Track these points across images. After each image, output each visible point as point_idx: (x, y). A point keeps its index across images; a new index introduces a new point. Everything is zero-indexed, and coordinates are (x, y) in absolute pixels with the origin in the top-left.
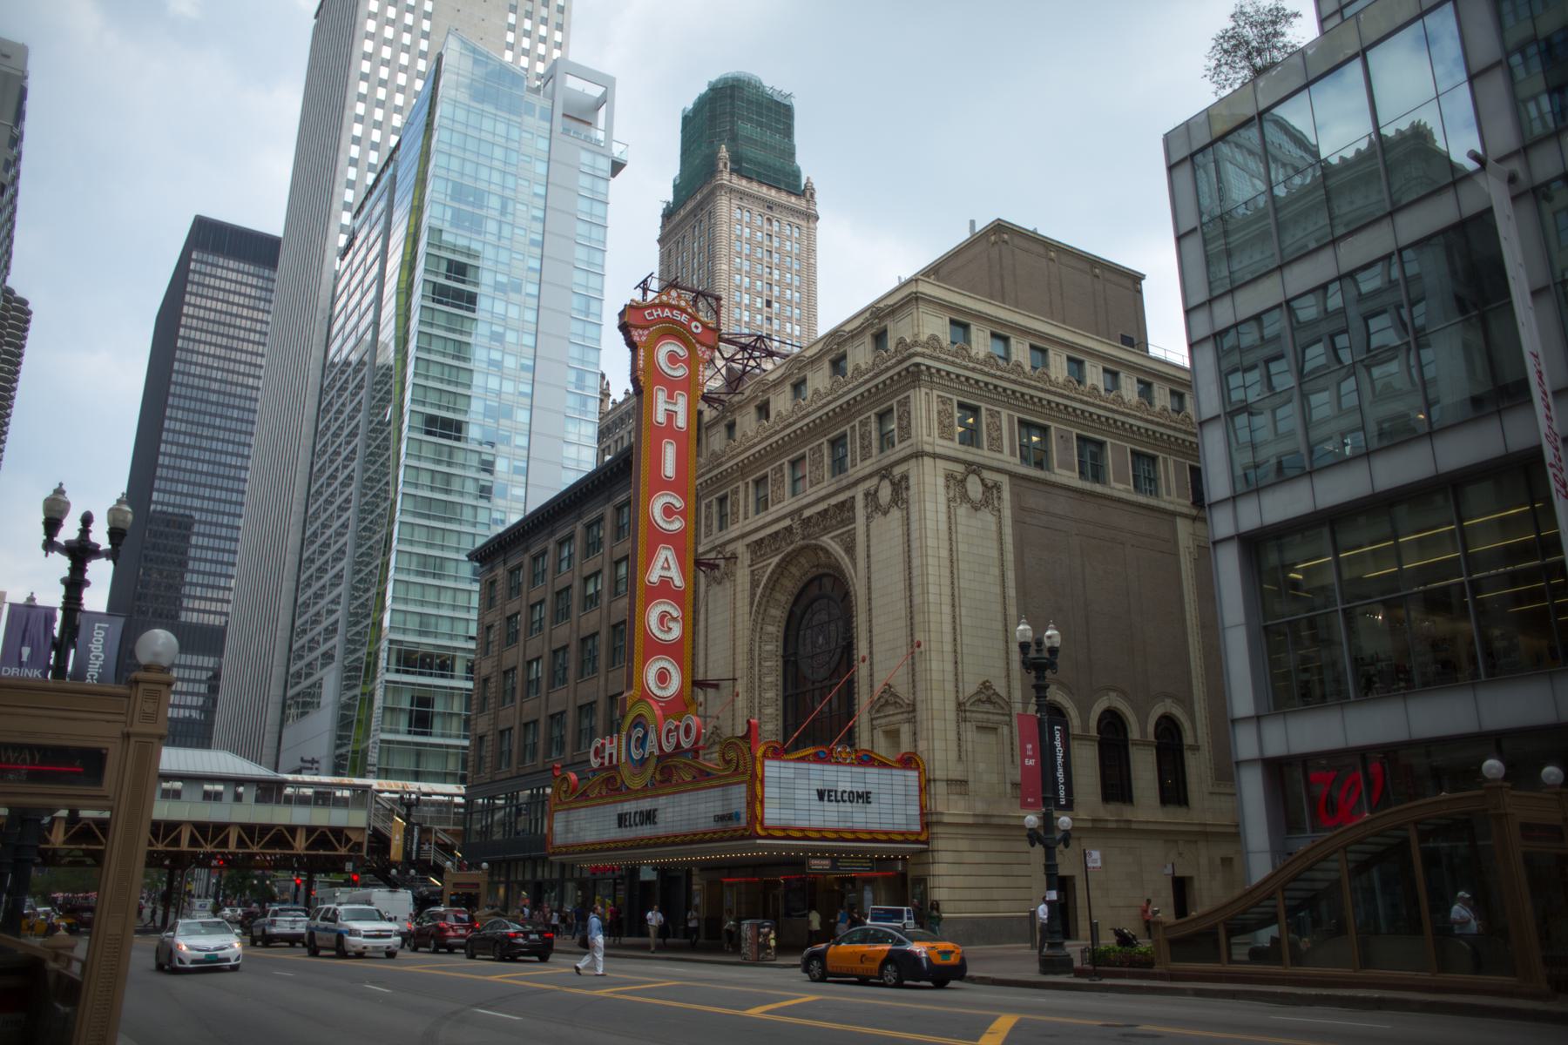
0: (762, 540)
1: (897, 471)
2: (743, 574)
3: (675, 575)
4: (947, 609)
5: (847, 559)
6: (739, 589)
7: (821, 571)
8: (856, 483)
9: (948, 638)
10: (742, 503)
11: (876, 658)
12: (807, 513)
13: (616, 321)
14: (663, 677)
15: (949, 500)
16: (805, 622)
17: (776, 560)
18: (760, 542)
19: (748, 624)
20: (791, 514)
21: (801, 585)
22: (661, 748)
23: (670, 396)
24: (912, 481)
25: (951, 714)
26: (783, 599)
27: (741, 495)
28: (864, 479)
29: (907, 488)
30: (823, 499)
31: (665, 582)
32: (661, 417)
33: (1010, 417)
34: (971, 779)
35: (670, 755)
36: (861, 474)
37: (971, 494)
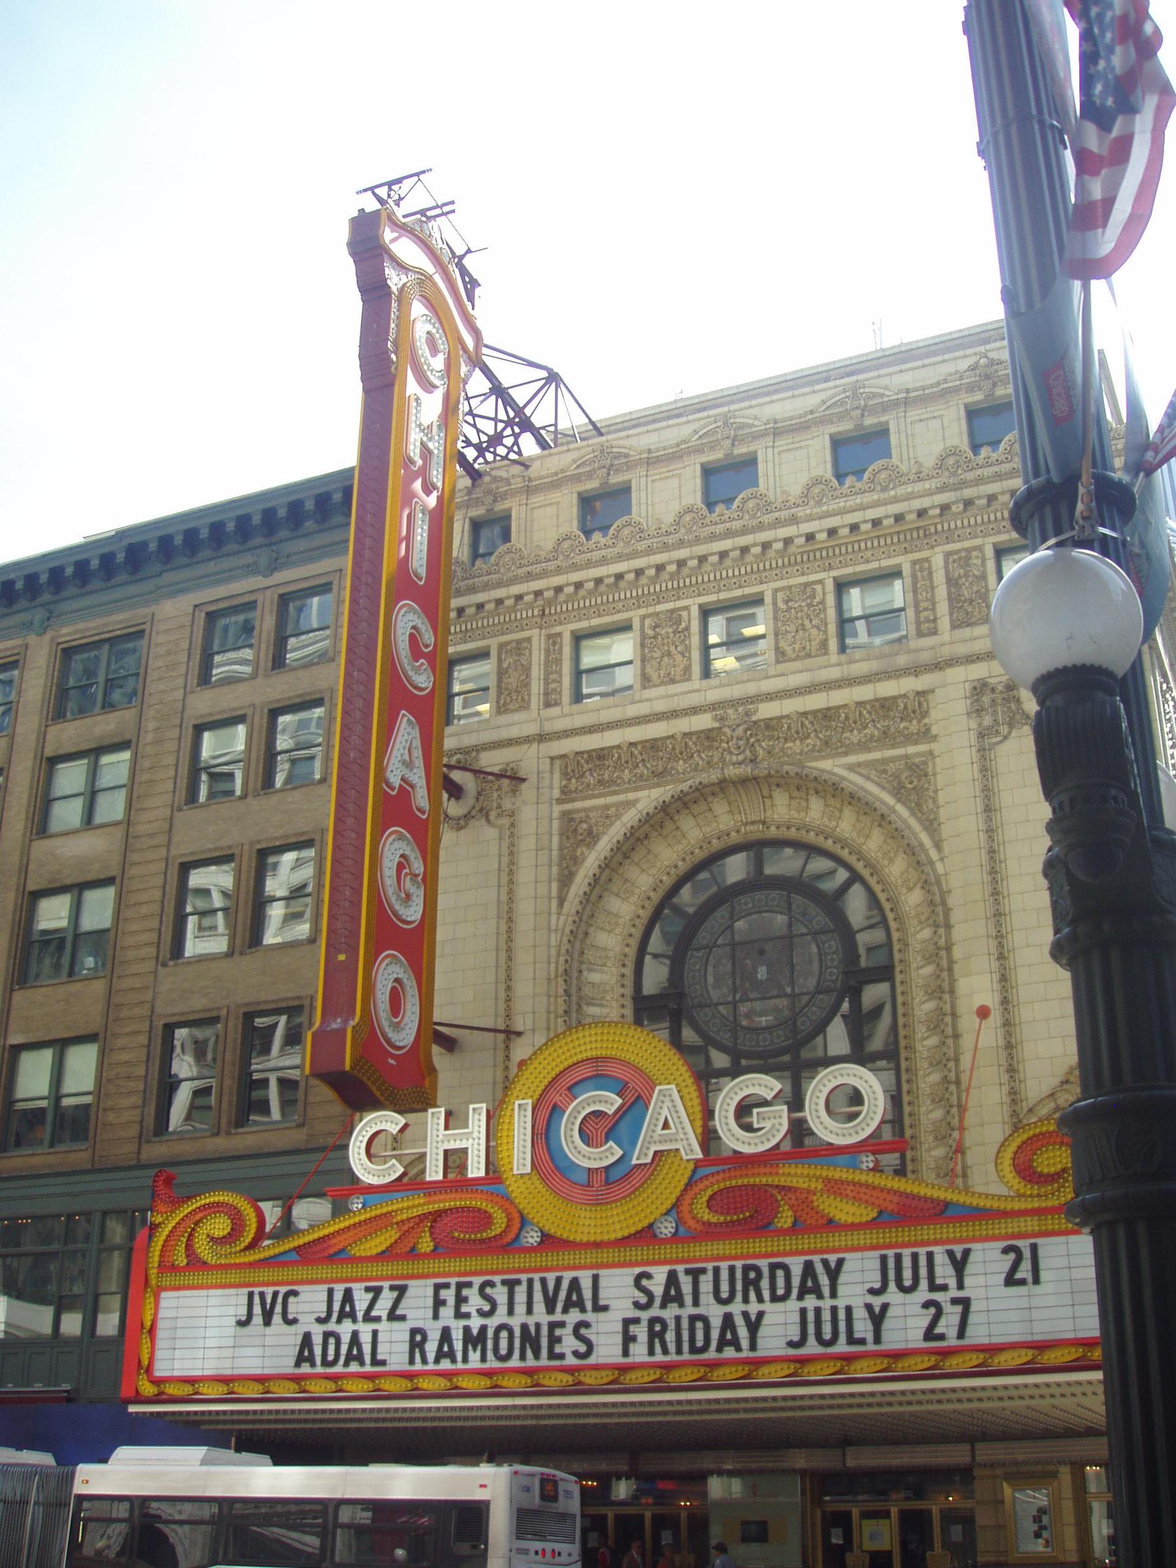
2: (536, 815)
3: (418, 777)
5: (901, 809)
6: (527, 845)
8: (951, 662)
10: (536, 672)
11: (1025, 1014)
12: (767, 710)
13: (343, 234)
16: (703, 936)
17: (649, 798)
18: (600, 756)
19: (563, 921)
20: (713, 707)
21: (700, 855)
22: (709, 1137)
27: (537, 659)
31: (405, 793)
35: (740, 1161)
36: (961, 650)
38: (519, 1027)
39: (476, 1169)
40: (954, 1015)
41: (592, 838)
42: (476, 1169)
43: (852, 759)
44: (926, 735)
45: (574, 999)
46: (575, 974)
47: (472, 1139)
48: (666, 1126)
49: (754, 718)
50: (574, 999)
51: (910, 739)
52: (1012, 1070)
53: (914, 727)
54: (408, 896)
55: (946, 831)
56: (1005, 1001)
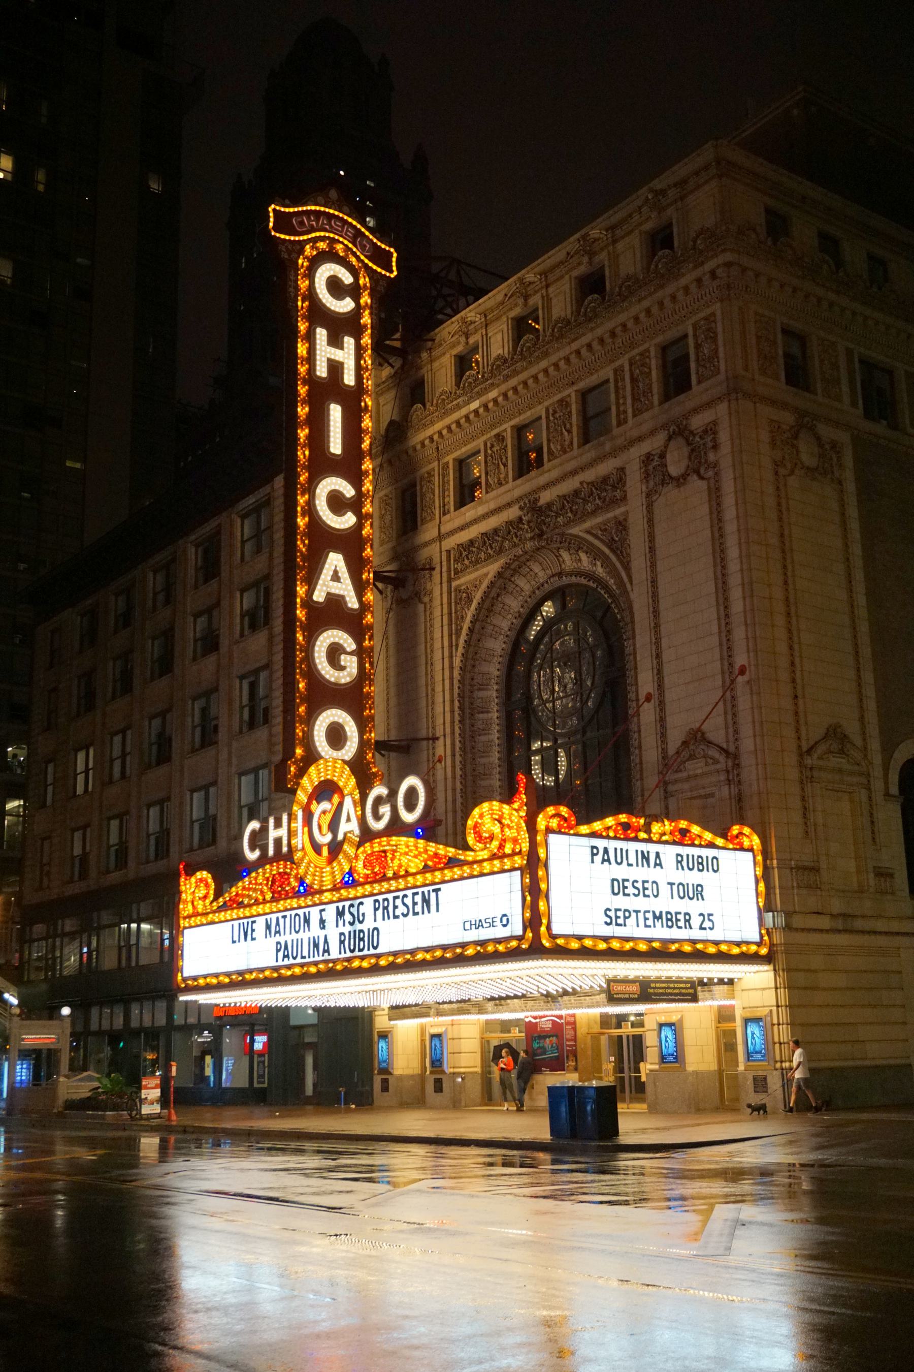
0: (471, 542)
1: (697, 422)
3: (346, 589)
4: (780, 620)
7: (565, 580)
9: (784, 662)
11: (669, 696)
12: (546, 497)
14: (336, 736)
15: (775, 463)
23: (335, 341)
24: (724, 436)
25: (793, 774)
26: (505, 625)
28: (640, 439)
29: (715, 447)
30: (574, 473)
31: (335, 601)
32: (322, 371)
33: (849, 352)
34: (824, 866)
36: (635, 433)
37: (805, 458)
38: (438, 735)
39: (285, 849)
40: (637, 700)
41: (470, 600)
42: (285, 849)
43: (587, 525)
44: (624, 498)
45: (468, 711)
46: (467, 694)
47: (283, 832)
48: (348, 820)
49: (539, 504)
50: (468, 711)
51: (615, 502)
52: (663, 735)
53: (618, 494)
54: (343, 668)
55: (634, 570)
56: (660, 686)
